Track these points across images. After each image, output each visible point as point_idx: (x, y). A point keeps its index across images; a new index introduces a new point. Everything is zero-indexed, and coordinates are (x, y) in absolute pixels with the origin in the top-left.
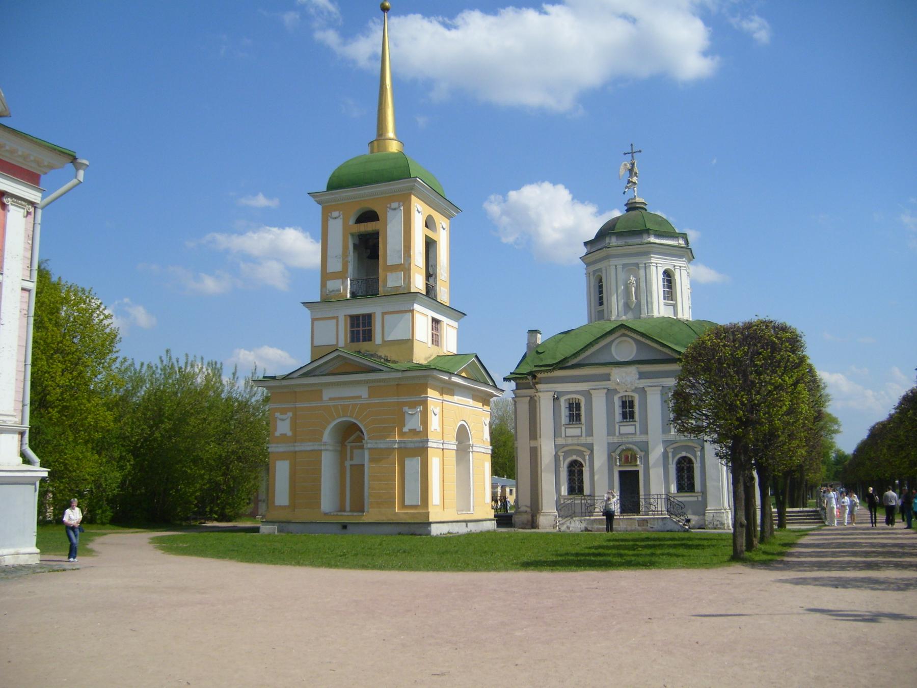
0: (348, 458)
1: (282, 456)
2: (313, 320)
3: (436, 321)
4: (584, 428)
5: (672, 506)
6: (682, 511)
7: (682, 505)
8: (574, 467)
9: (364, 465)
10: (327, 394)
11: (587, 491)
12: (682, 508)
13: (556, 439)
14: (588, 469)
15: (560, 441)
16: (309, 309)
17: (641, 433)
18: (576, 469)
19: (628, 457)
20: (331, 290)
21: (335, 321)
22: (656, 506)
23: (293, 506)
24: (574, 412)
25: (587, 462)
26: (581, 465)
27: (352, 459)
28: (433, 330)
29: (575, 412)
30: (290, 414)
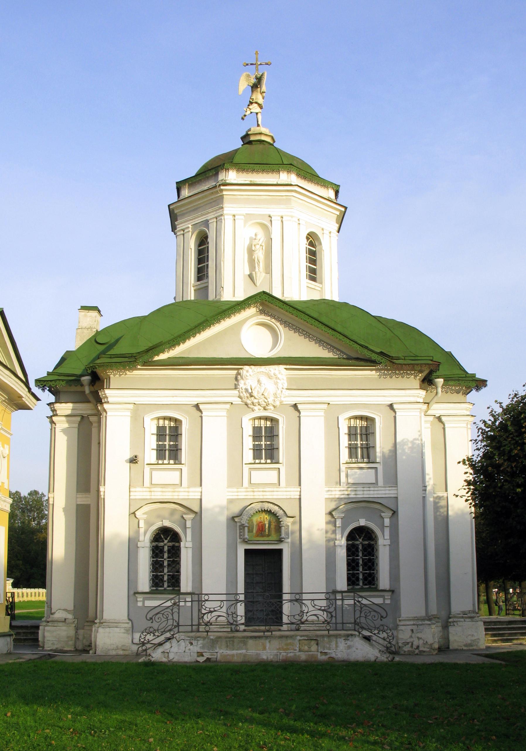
4: (185, 469)
5: (363, 615)
6: (381, 623)
7: (384, 614)
12: (382, 617)
13: (131, 490)
14: (190, 544)
15: (140, 493)
17: (288, 485)
19: (265, 525)
22: (334, 614)
24: (167, 443)
25: (189, 532)
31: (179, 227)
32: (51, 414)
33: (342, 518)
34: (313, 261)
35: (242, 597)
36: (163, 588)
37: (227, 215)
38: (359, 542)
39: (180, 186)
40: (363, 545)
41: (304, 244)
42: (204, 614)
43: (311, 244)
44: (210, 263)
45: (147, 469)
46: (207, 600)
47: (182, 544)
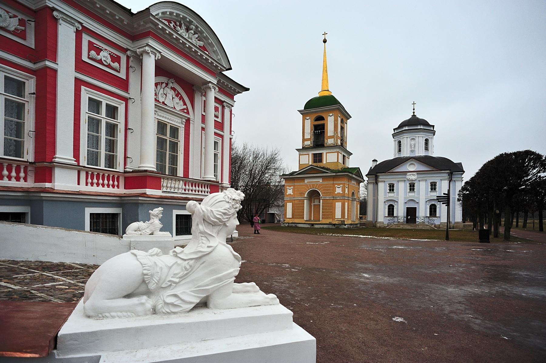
0: (313, 202)
1: (290, 201)
2: (300, 155)
3: (344, 156)
10: (306, 181)
11: (395, 215)
21: (308, 155)
23: (293, 217)
26: (393, 206)
27: (314, 203)
29: (392, 188)
30: (292, 187)
35: (406, 217)
38: (433, 207)
45: (387, 193)
47: (394, 207)
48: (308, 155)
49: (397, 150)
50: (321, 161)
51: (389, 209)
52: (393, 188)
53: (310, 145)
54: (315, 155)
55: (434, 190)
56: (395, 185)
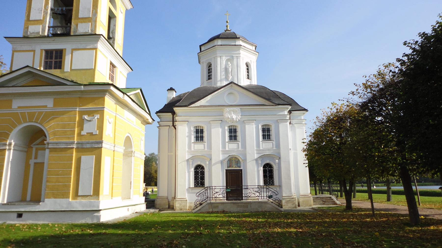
2: (14, 51)
4: (206, 144)
7: (277, 194)
8: (199, 169)
9: (44, 163)
11: (207, 184)
12: (276, 194)
16: (11, 44)
18: (199, 170)
20: (32, 32)
21: (33, 53)
26: (203, 168)
28: (110, 71)
31: (201, 61)
32: (158, 126)
33: (261, 160)
34: (248, 72)
36: (199, 186)
37: (218, 56)
39: (200, 46)
40: (269, 170)
41: (245, 66)
42: (214, 194)
43: (247, 66)
44: (212, 73)
45: (192, 144)
46: (215, 189)
48: (33, 53)
49: (213, 67)
50: (59, 65)
51: (196, 173)
52: (203, 134)
53: (40, 33)
54: (49, 53)
55: (268, 139)
56: (205, 130)
